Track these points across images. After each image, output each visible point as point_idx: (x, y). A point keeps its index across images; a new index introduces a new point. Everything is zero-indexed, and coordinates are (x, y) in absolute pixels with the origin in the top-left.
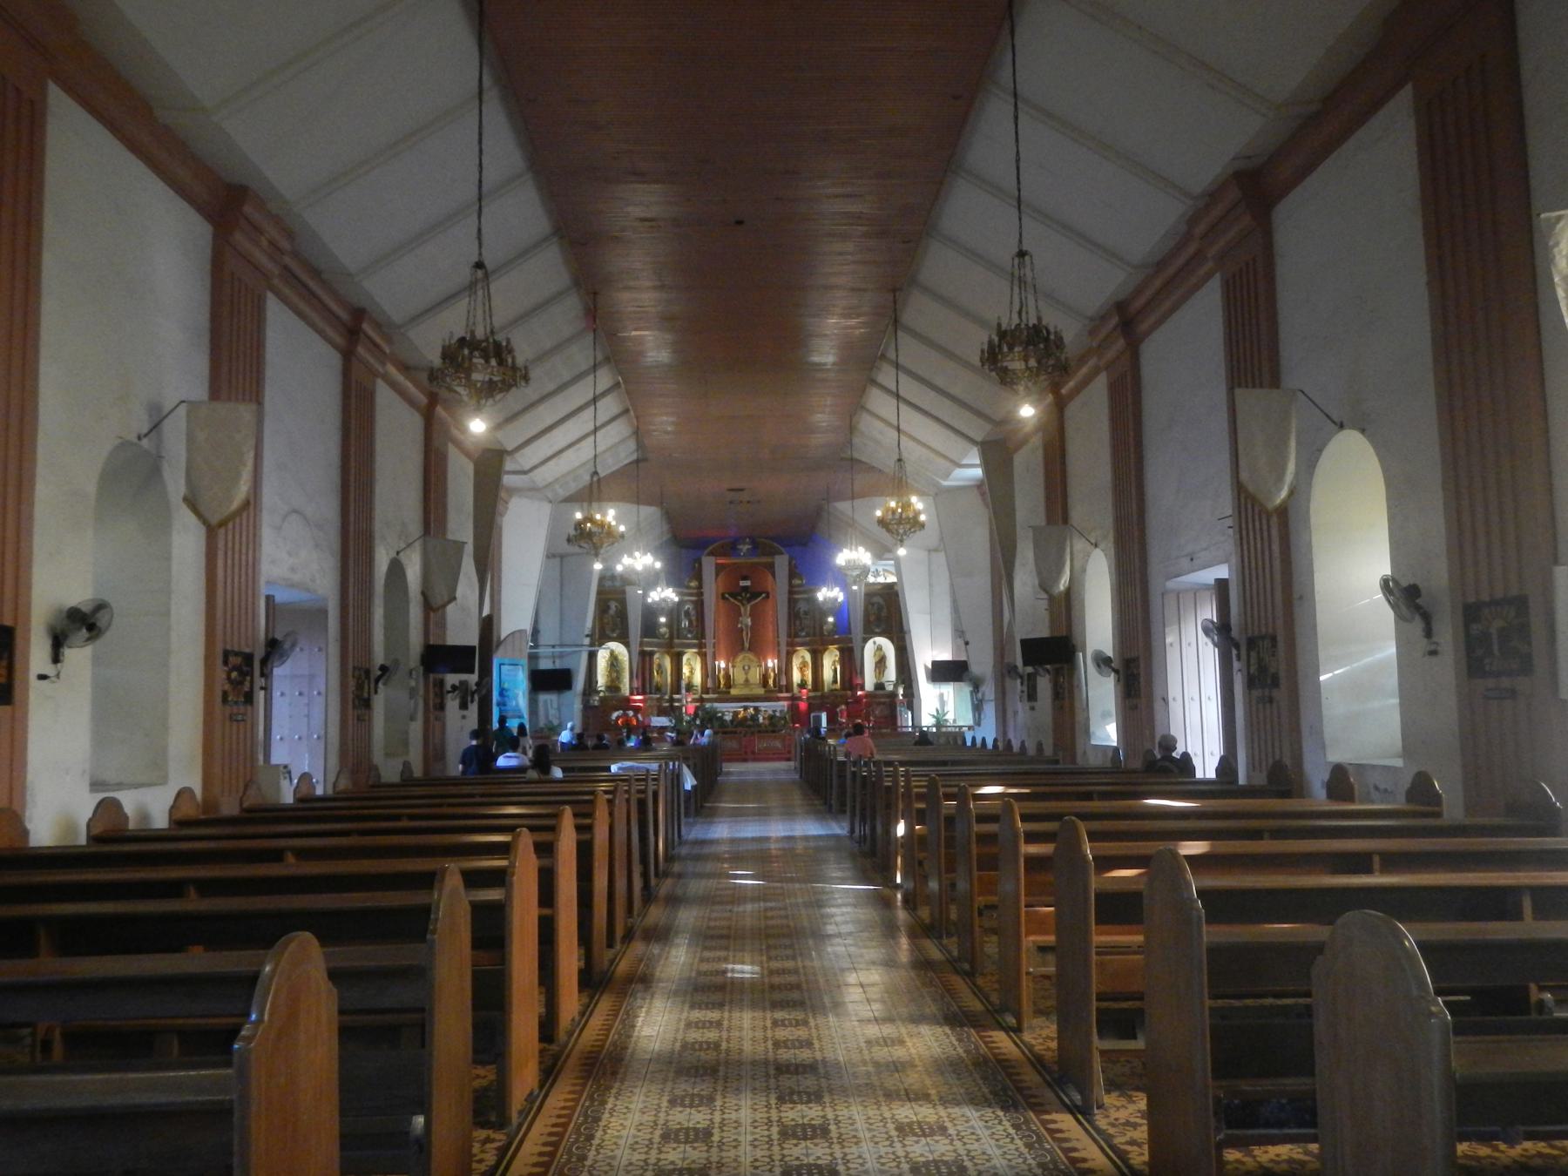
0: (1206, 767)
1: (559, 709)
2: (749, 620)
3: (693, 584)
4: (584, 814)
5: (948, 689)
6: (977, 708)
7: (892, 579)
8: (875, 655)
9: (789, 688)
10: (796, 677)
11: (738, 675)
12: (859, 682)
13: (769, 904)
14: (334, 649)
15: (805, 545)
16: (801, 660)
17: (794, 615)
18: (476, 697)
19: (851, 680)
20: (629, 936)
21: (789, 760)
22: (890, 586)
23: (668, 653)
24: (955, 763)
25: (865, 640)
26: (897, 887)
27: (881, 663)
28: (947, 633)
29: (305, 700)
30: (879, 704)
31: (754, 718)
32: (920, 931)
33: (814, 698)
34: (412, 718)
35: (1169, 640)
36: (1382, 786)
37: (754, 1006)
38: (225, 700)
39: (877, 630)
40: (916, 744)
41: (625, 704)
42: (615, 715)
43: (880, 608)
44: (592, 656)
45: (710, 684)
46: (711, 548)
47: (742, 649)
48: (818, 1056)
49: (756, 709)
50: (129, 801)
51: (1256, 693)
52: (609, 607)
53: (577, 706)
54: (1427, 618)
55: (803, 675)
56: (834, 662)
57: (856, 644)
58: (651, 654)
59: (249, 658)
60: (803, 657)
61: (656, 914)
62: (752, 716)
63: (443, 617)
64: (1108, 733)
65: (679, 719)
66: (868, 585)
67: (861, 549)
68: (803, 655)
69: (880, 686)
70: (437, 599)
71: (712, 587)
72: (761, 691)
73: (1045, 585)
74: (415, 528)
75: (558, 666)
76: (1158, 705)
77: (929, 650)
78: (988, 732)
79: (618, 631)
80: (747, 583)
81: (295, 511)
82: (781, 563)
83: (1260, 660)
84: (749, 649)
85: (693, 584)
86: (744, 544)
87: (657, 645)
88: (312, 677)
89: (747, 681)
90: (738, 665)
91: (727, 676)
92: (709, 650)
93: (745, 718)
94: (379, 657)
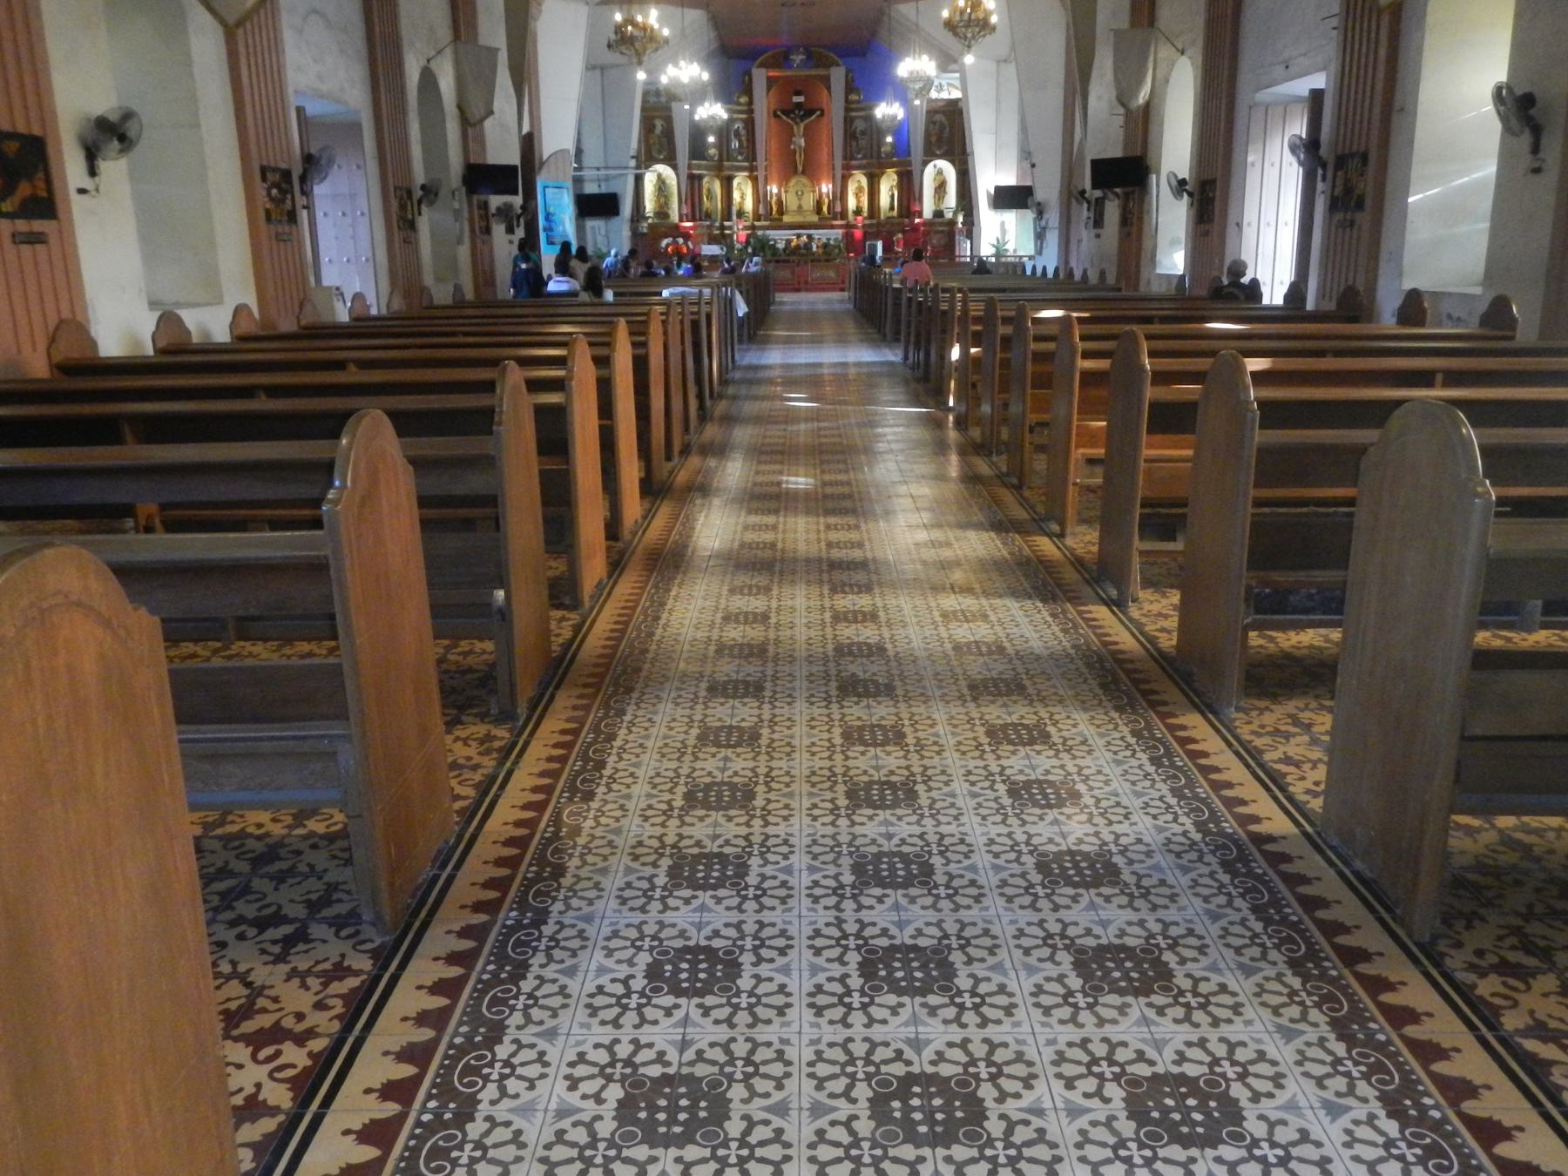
0: (1274, 294)
1: (607, 236)
3: (743, 100)
4: (639, 331)
5: (1010, 217)
6: (1040, 236)
7: (957, 94)
9: (844, 214)
10: (852, 204)
11: (791, 201)
13: (823, 424)
14: (372, 166)
15: (864, 55)
17: (850, 135)
18: (522, 221)
19: (908, 208)
20: (686, 451)
21: (842, 290)
22: (956, 101)
24: (1014, 290)
25: (925, 163)
26: (950, 409)
27: (941, 188)
28: (1012, 154)
29: (348, 220)
30: (937, 232)
31: (807, 246)
32: (970, 449)
33: (870, 226)
34: (460, 242)
35: (1250, 159)
36: (1456, 315)
37: (808, 512)
38: (269, 219)
40: (974, 272)
41: (675, 231)
42: (664, 242)
43: (942, 131)
44: (639, 180)
45: (761, 211)
47: (795, 172)
48: (869, 555)
49: (810, 237)
50: (190, 318)
51: (1339, 216)
52: (654, 126)
53: (626, 233)
54: (1537, 130)
55: (858, 201)
57: (915, 168)
58: (700, 177)
59: (286, 175)
61: (711, 432)
63: (482, 130)
64: (1174, 261)
65: (731, 247)
66: (930, 101)
67: (925, 57)
68: (859, 180)
69: (938, 214)
70: (476, 112)
71: (763, 102)
72: (815, 218)
73: (1123, 100)
74: (444, 32)
75: (604, 190)
76: (1231, 230)
77: (992, 174)
78: (1050, 261)
80: (801, 99)
81: (315, 11)
82: (838, 75)
83: (1347, 181)
84: (803, 172)
85: (743, 100)
87: (706, 168)
88: (353, 196)
89: (800, 207)
91: (780, 203)
92: (760, 174)
93: (798, 247)
94: (419, 176)
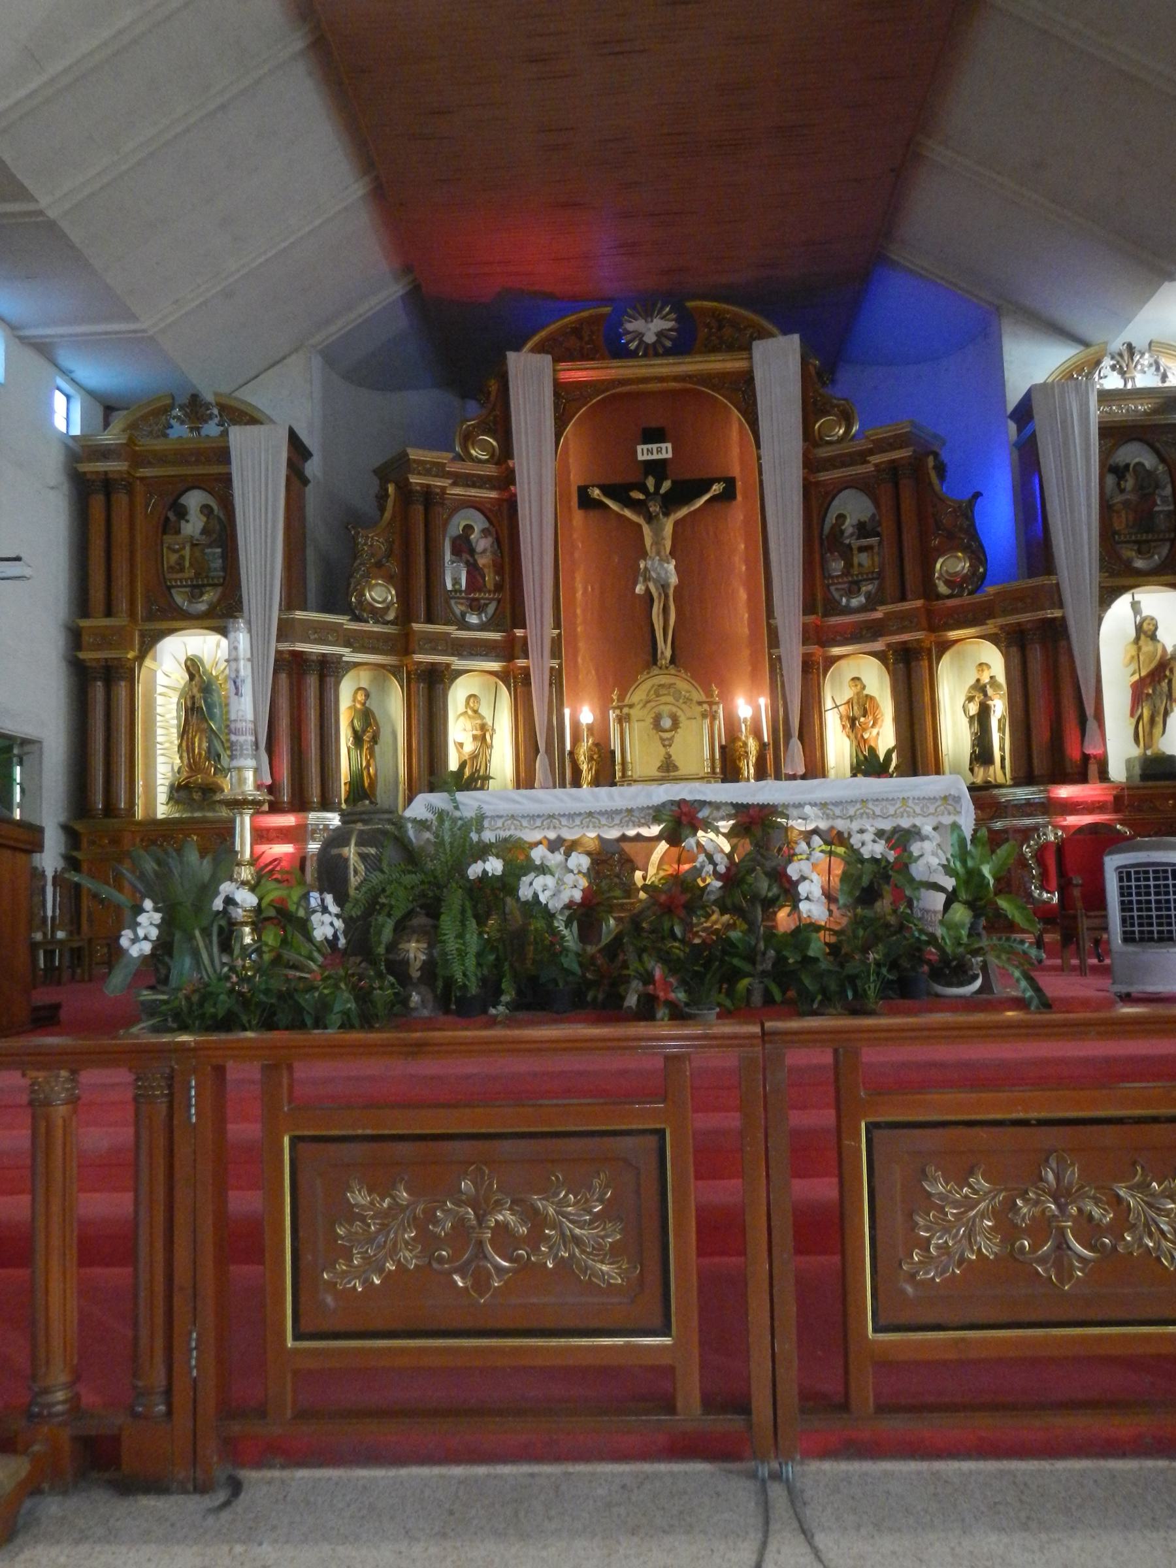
2: (671, 566)
8: (1139, 649)
12: (1089, 750)
16: (848, 693)
23: (395, 671)
25: (1108, 596)
39: (1139, 564)
46: (543, 334)
52: (182, 513)
55: (860, 742)
56: (980, 688)
57: (1074, 612)
60: (856, 679)
62: (732, 878)
66: (1106, 396)
79: (210, 596)
80: (664, 451)
86: (648, 315)
87: (351, 640)
90: (635, 713)
92: (539, 664)
